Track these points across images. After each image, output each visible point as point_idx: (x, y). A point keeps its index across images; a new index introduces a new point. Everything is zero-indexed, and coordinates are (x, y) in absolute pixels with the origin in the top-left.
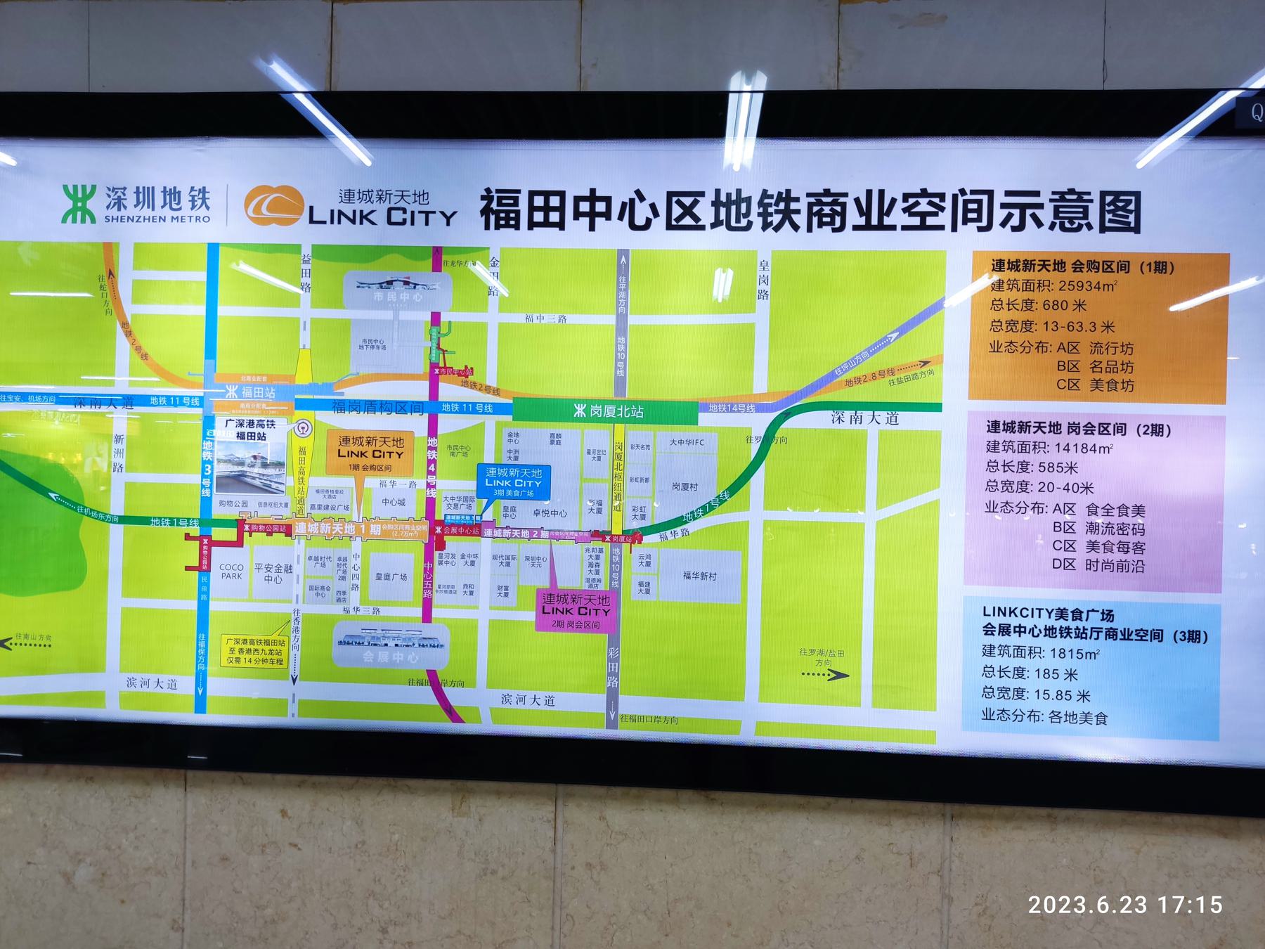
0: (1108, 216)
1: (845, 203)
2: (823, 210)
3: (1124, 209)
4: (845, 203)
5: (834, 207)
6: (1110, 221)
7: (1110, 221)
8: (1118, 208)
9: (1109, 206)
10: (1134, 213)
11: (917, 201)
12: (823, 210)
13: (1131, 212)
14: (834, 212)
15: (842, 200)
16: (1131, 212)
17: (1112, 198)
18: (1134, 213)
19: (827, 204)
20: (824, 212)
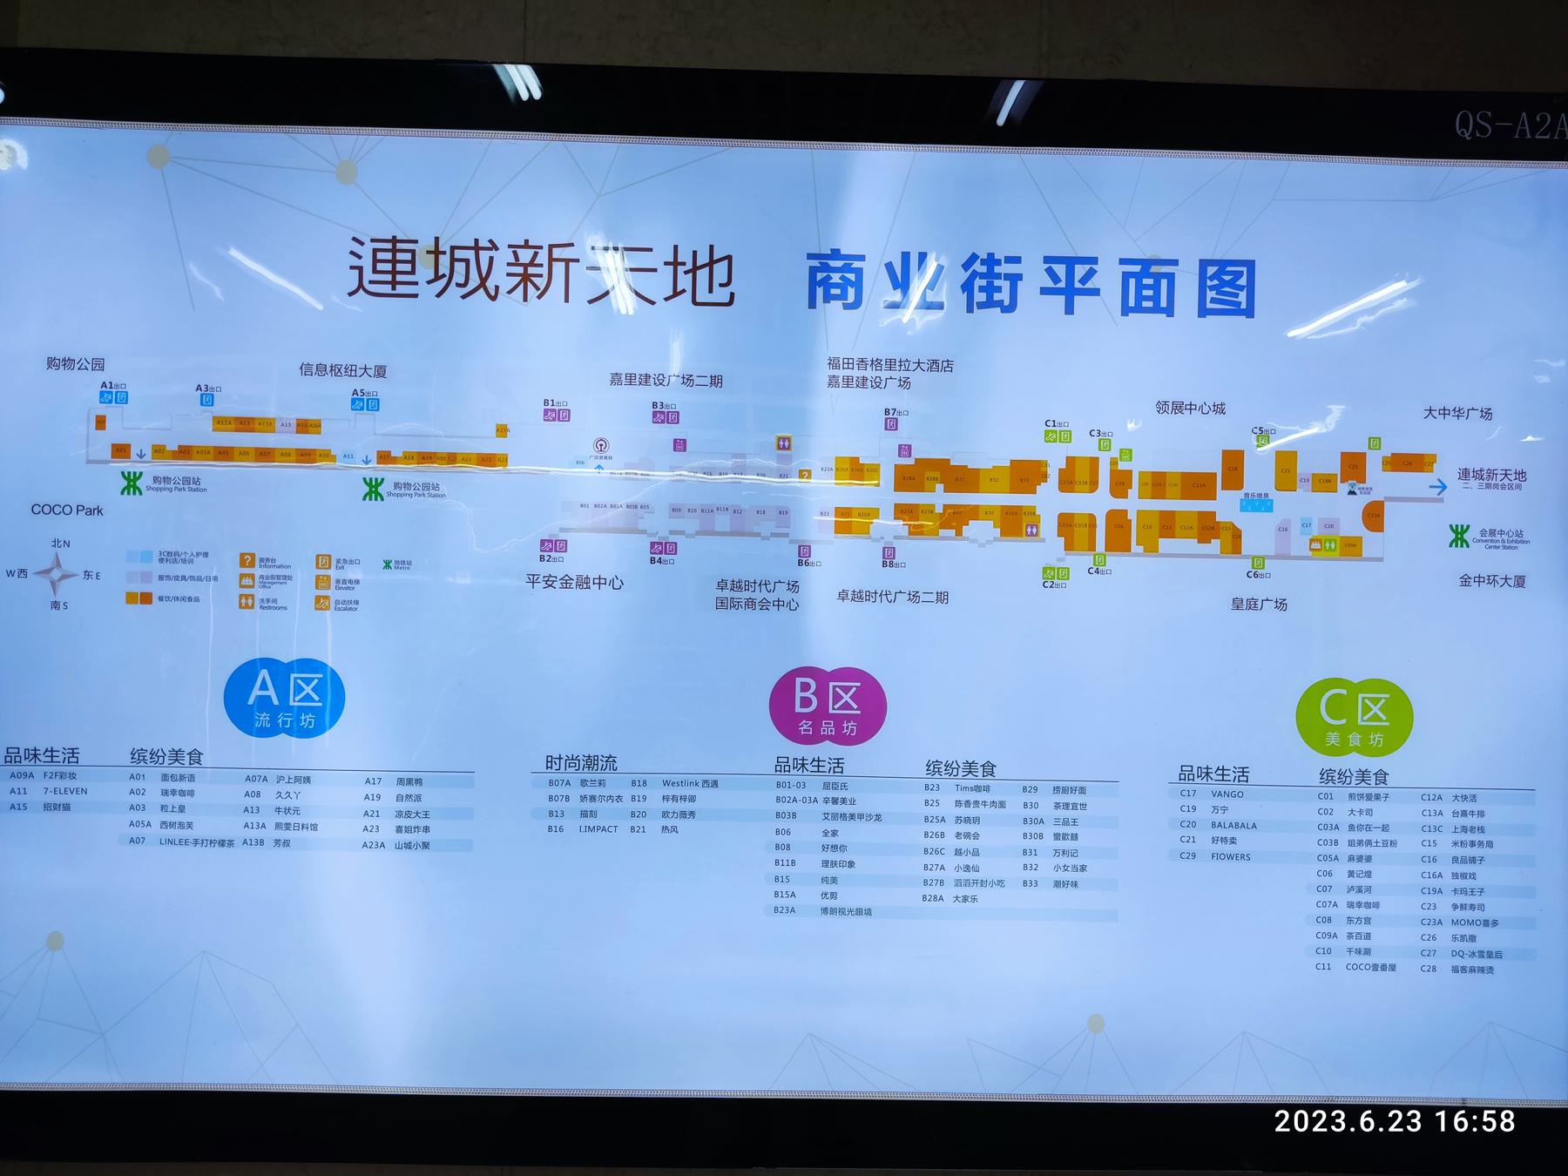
0: (1211, 294)
1: (861, 270)
2: (831, 278)
3: (1231, 284)
4: (861, 270)
6: (1213, 300)
7: (1213, 300)
8: (1223, 283)
9: (1211, 281)
10: (1245, 290)
11: (1050, 267)
12: (831, 278)
13: (1241, 288)
14: (846, 283)
15: (856, 264)
16: (1241, 288)
17: (1216, 268)
18: (1245, 290)
19: (836, 270)
20: (831, 281)
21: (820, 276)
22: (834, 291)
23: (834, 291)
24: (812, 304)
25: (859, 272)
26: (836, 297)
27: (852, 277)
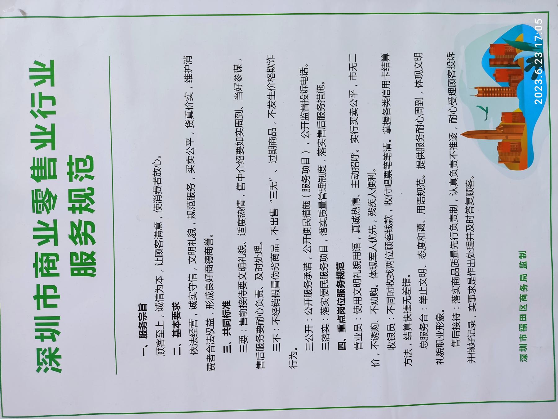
5: (44, 261)
14: (47, 260)
15: (39, 256)
21: (45, 272)
22: (51, 266)
23: (51, 266)
24: (57, 275)
25: (43, 255)
26: (54, 264)
27: (45, 258)
